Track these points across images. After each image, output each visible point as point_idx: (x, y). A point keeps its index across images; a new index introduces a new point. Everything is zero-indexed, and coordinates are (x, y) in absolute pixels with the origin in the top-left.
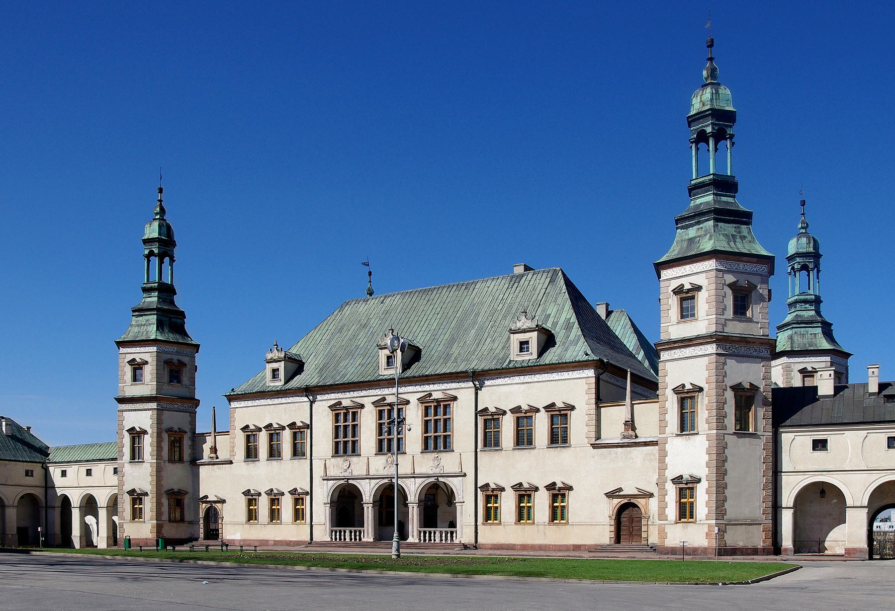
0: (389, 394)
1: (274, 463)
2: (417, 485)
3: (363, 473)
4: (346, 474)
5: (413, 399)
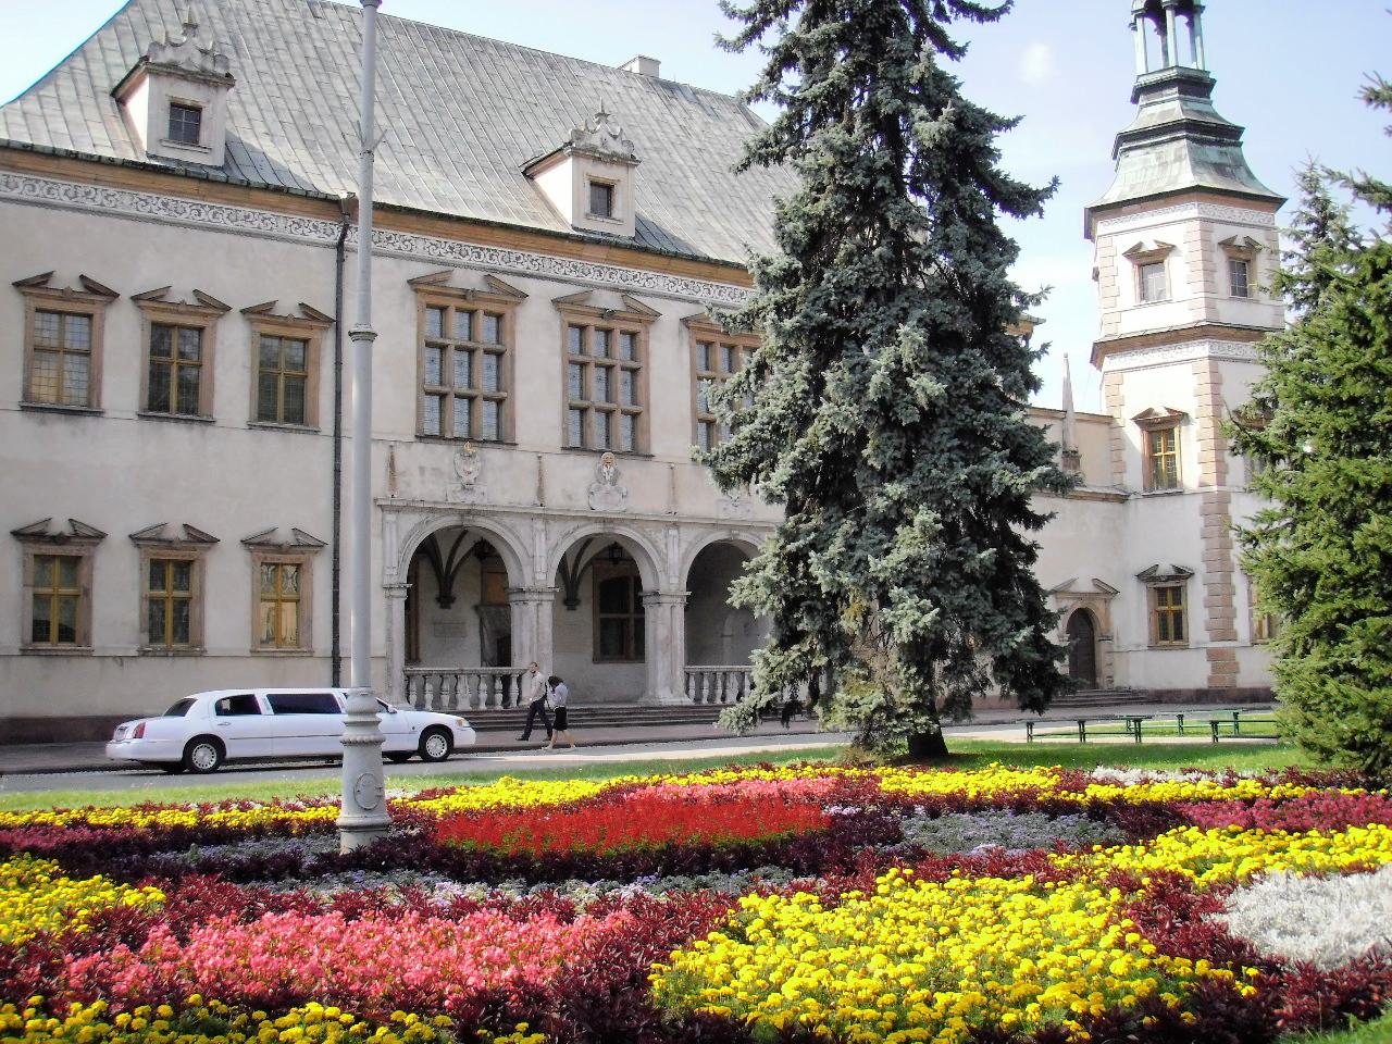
0: (605, 282)
1: (176, 437)
2: (684, 545)
3: (525, 495)
4: (470, 498)
5: (671, 313)
